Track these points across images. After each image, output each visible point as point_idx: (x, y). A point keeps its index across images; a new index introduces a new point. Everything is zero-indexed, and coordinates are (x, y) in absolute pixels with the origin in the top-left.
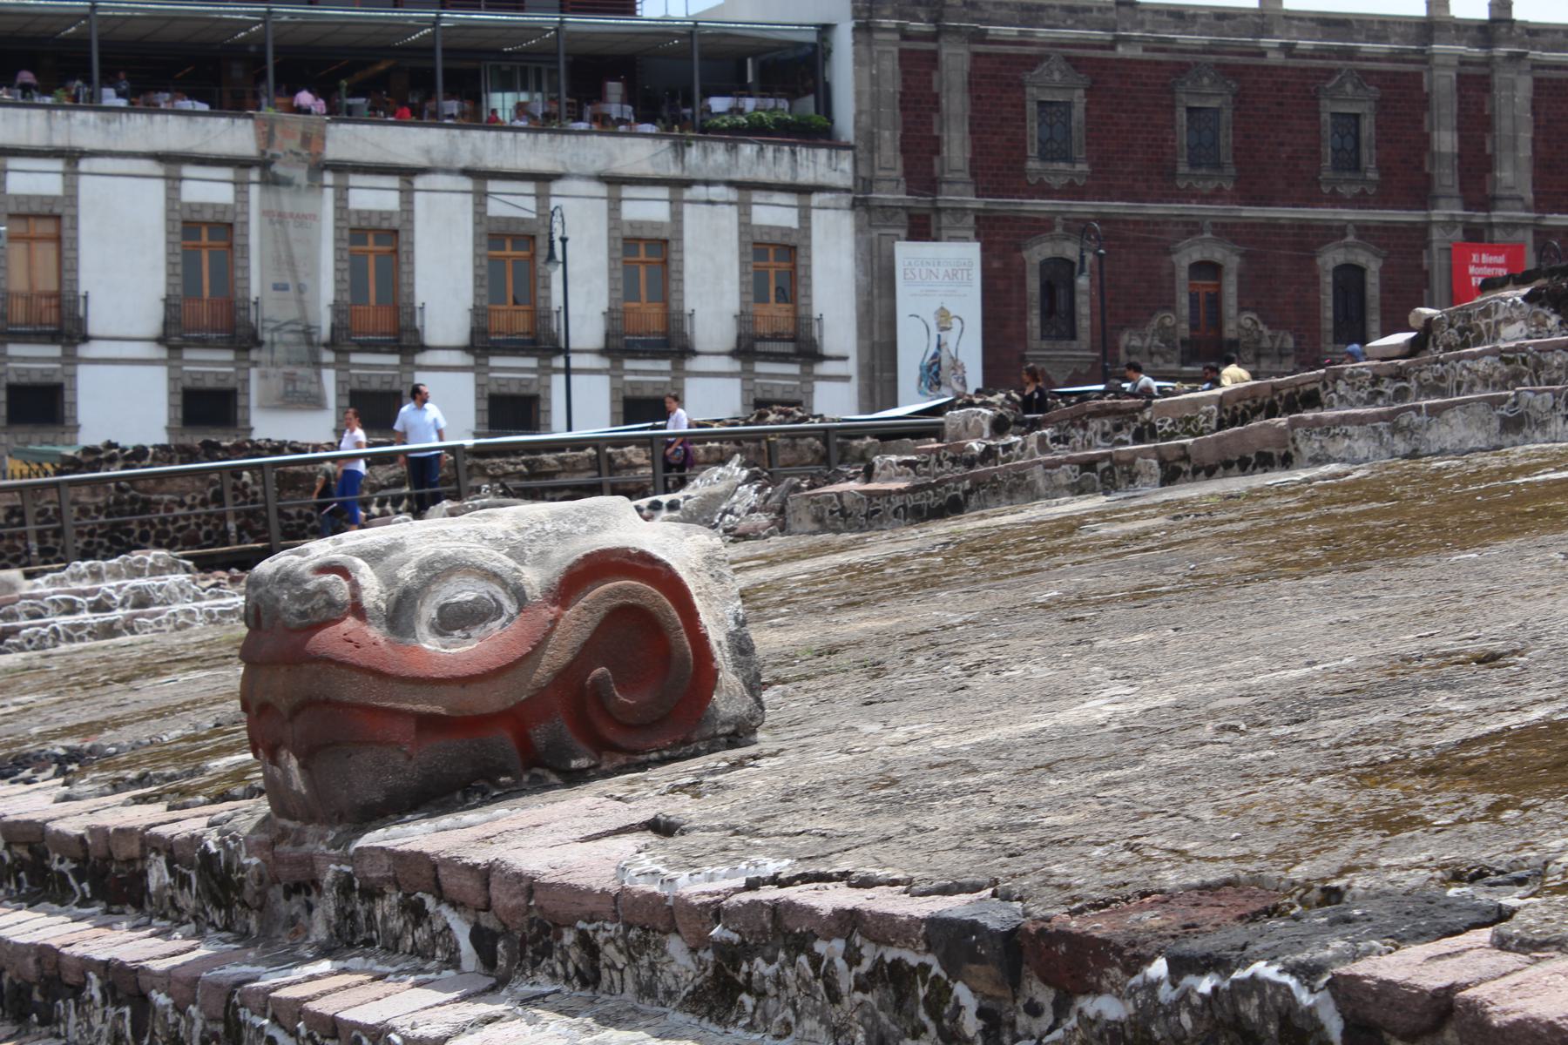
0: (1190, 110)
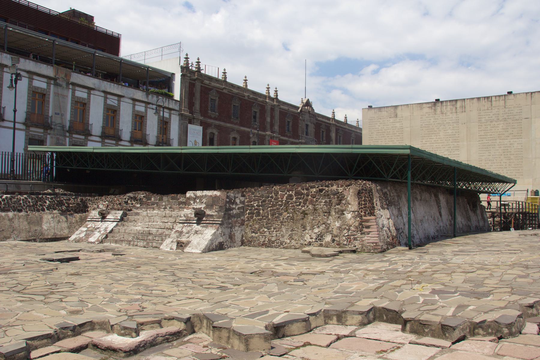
0: (234, 105)
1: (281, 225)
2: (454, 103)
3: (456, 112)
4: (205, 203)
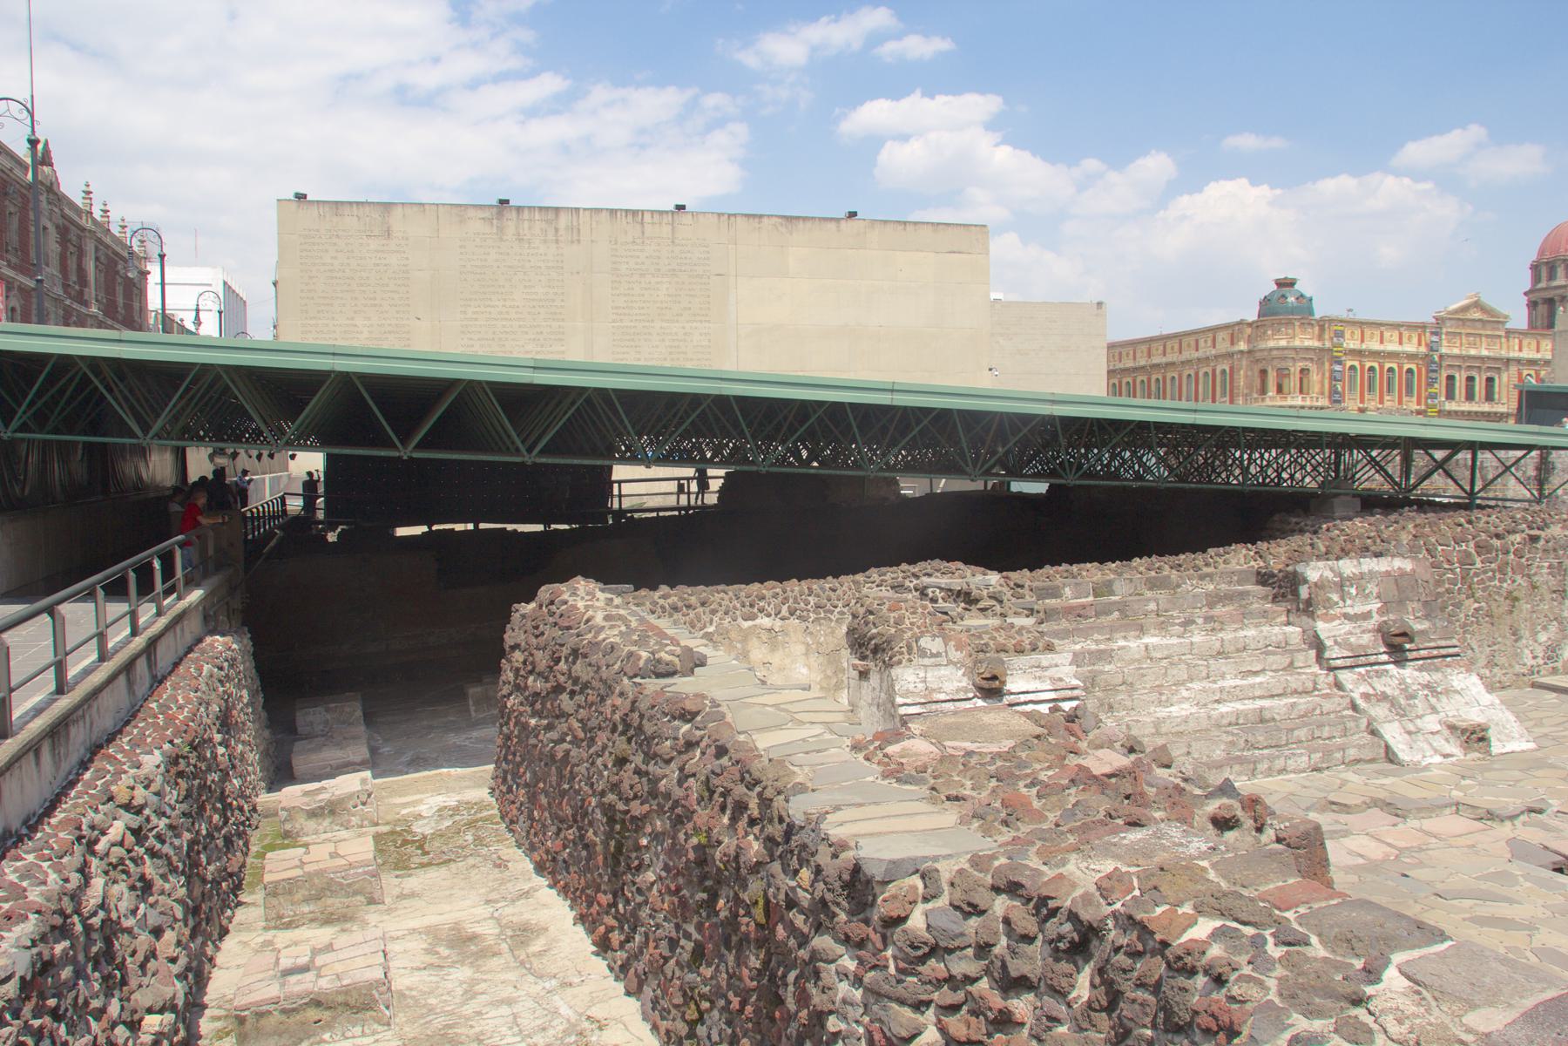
1: (1464, 633)
2: (551, 216)
3: (557, 242)
4: (1378, 597)
